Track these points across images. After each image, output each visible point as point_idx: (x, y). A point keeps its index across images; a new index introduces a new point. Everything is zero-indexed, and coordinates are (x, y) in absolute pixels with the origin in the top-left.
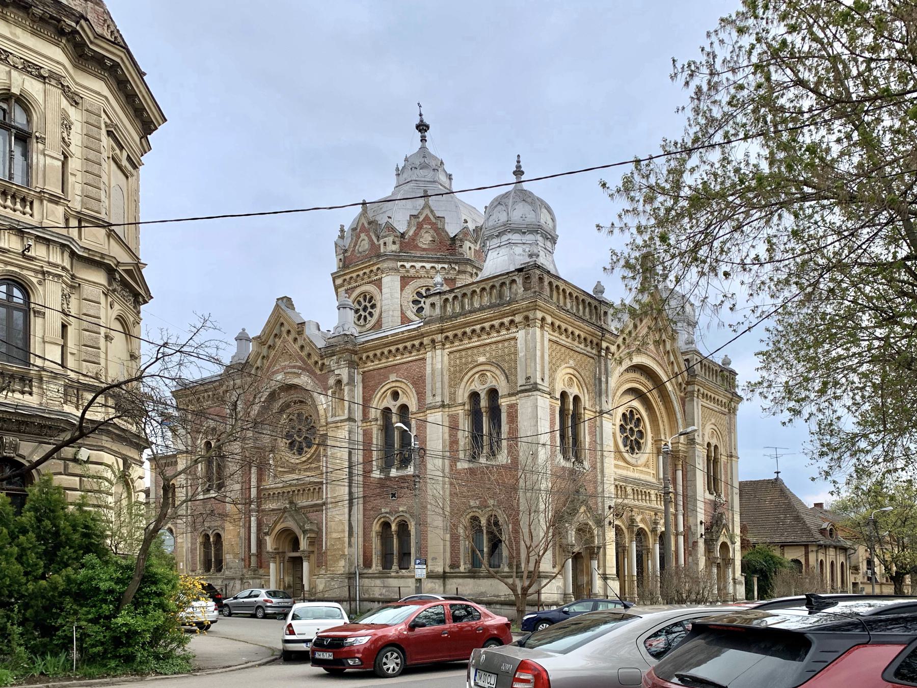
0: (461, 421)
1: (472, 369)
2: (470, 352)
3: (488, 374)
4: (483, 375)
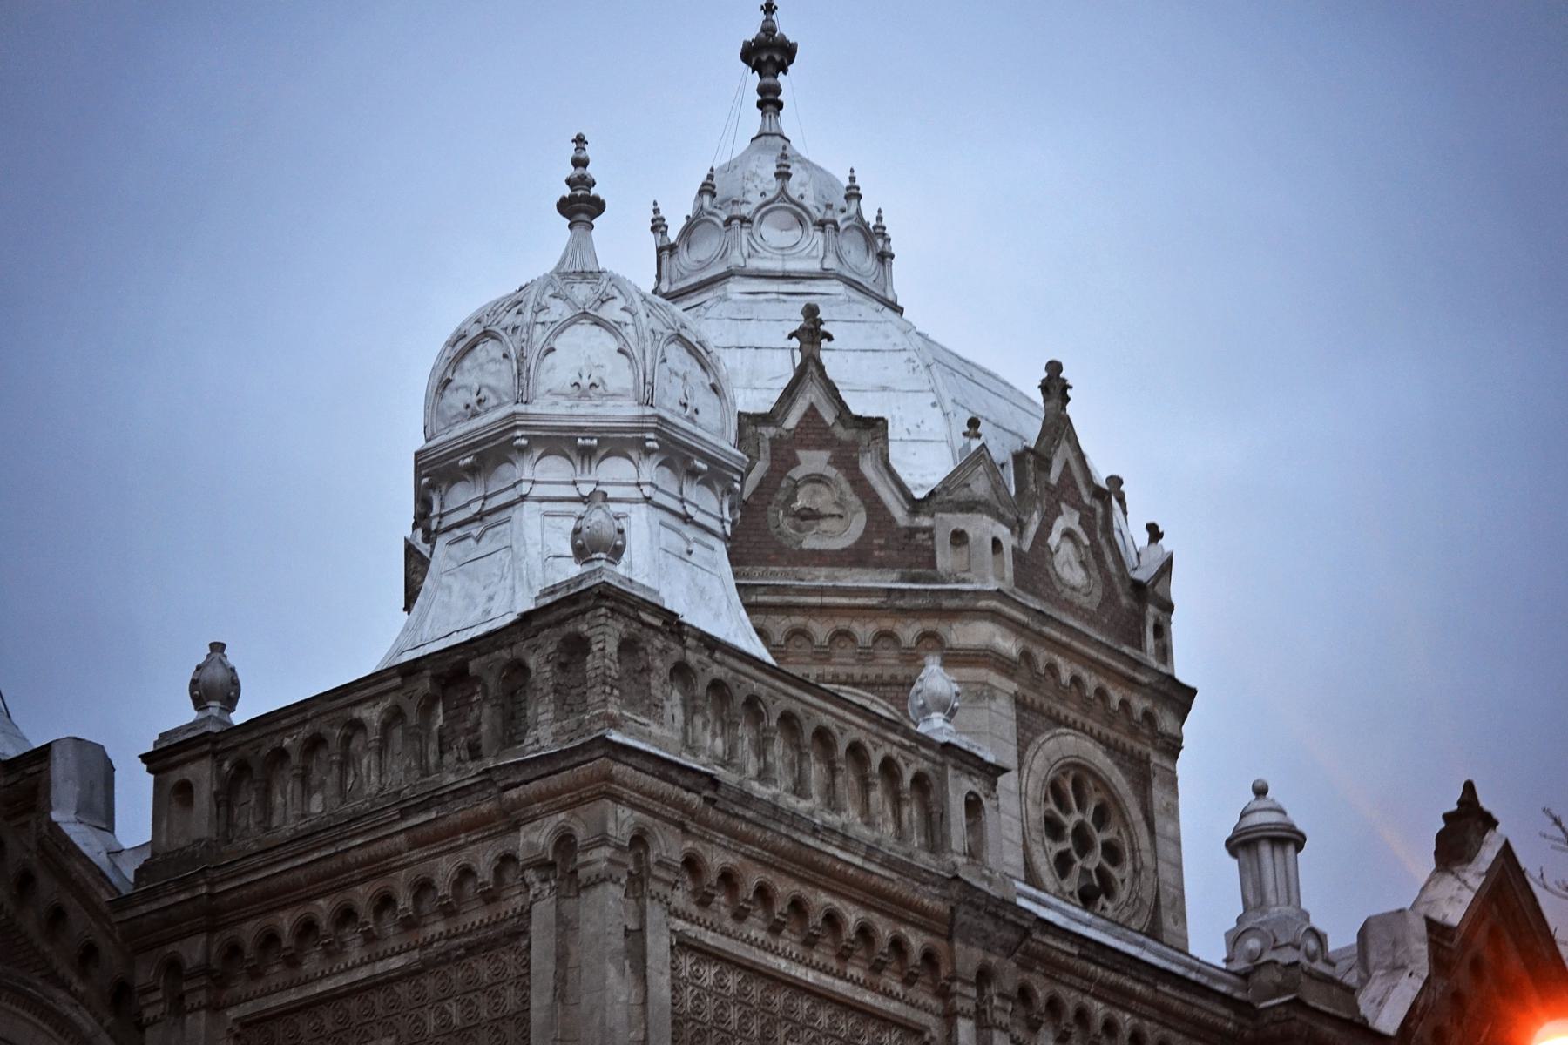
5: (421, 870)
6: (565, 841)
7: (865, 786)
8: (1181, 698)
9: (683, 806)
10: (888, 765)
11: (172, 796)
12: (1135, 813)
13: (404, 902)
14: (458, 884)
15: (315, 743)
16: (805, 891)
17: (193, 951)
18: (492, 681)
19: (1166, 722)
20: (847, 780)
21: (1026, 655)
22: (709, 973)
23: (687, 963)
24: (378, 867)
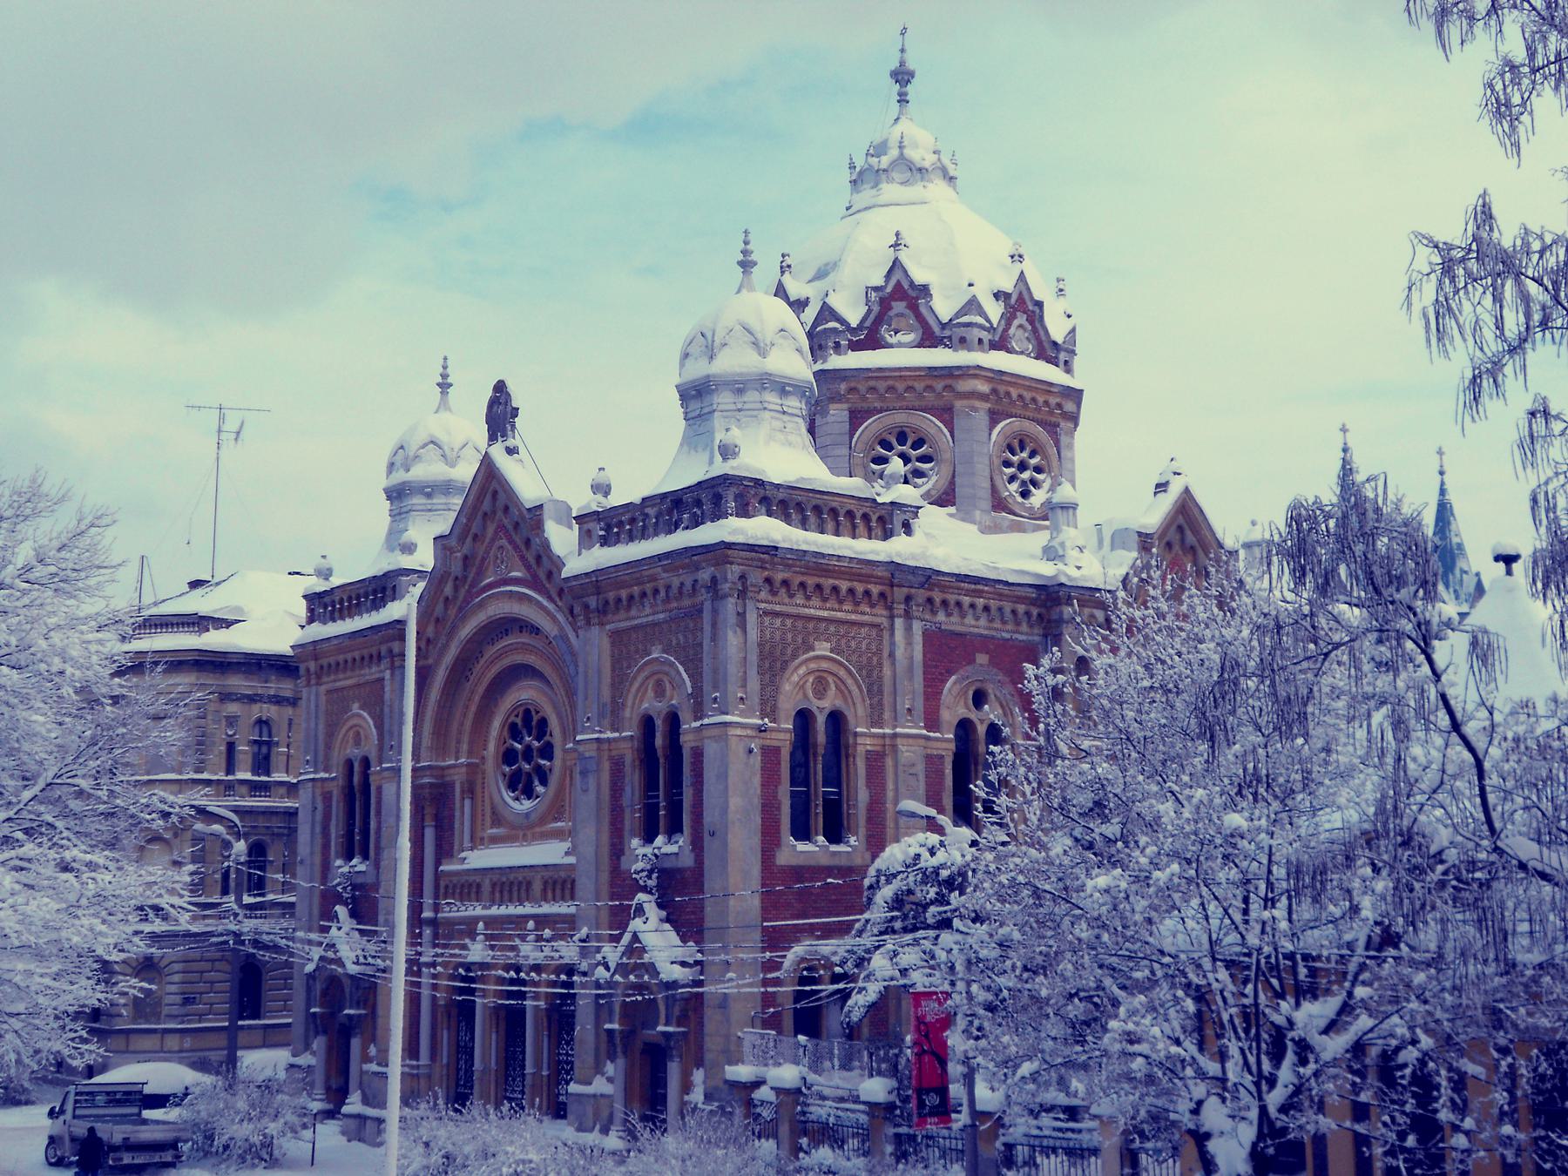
0: (628, 769)
6: (714, 580)
16: (822, 581)
21: (994, 391)
22: (778, 622)
24: (653, 579)
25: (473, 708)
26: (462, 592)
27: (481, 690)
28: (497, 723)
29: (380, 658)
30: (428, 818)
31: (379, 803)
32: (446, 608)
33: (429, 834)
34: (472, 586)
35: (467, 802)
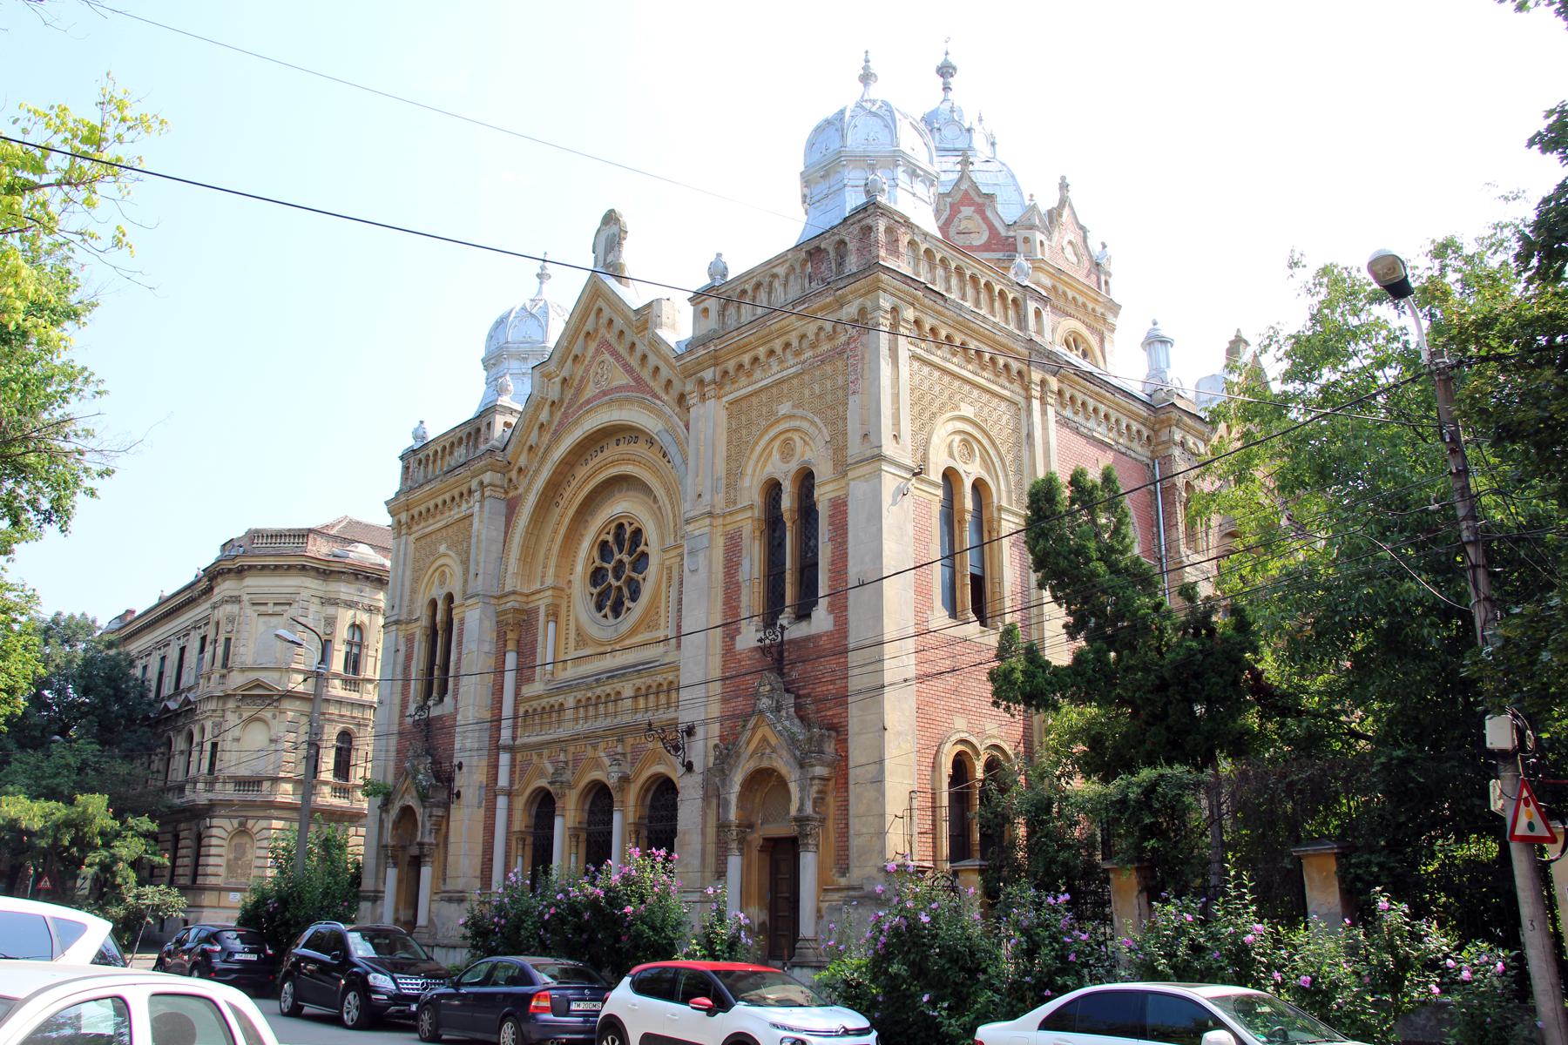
0: (746, 541)
1: (766, 430)
2: (764, 397)
3: (796, 437)
4: (787, 443)
5: (802, 331)
6: (862, 311)
7: (992, 300)
8: (1115, 308)
9: (915, 297)
10: (1001, 293)
11: (701, 313)
12: (1098, 353)
13: (795, 343)
14: (817, 334)
15: (758, 286)
16: (968, 339)
17: (708, 375)
18: (831, 250)
19: (1111, 318)
20: (984, 296)
21: (1054, 287)
22: (926, 370)
23: (916, 364)
25: (562, 530)
26: (558, 415)
27: (571, 512)
28: (586, 544)
29: (470, 492)
30: (511, 645)
31: (461, 634)
32: (540, 436)
33: (511, 660)
34: (569, 407)
35: (551, 625)
